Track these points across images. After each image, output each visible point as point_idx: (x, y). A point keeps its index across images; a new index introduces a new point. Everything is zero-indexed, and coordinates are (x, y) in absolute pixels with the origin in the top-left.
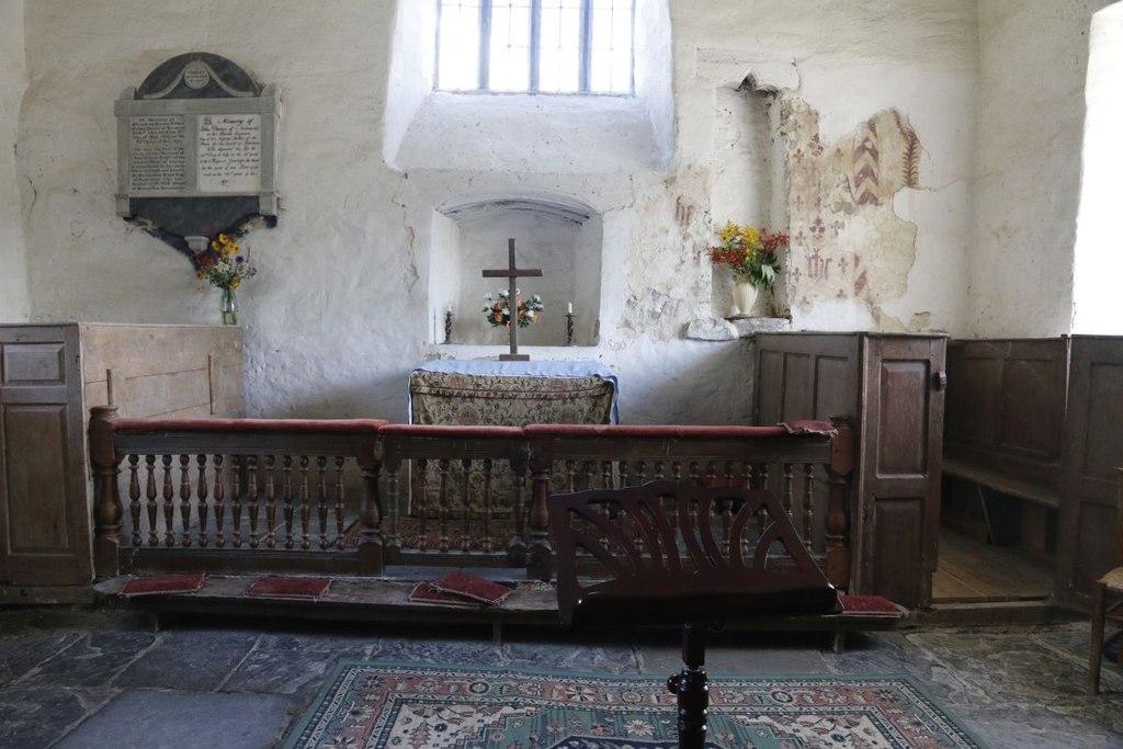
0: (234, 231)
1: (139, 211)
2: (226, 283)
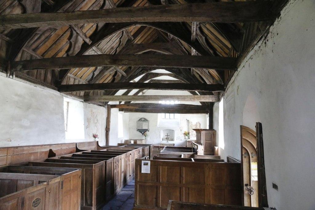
0: (146, 132)
1: (138, 130)
2: (145, 136)
